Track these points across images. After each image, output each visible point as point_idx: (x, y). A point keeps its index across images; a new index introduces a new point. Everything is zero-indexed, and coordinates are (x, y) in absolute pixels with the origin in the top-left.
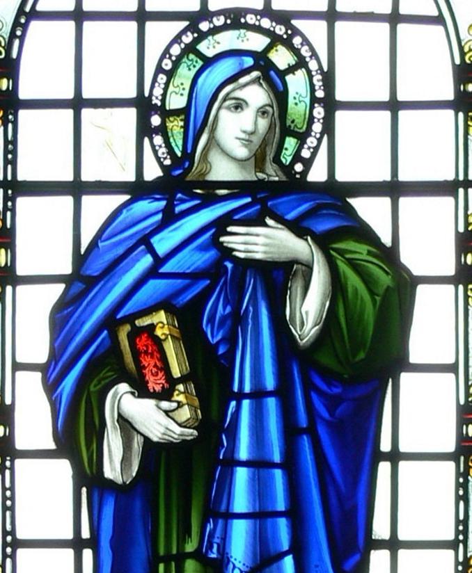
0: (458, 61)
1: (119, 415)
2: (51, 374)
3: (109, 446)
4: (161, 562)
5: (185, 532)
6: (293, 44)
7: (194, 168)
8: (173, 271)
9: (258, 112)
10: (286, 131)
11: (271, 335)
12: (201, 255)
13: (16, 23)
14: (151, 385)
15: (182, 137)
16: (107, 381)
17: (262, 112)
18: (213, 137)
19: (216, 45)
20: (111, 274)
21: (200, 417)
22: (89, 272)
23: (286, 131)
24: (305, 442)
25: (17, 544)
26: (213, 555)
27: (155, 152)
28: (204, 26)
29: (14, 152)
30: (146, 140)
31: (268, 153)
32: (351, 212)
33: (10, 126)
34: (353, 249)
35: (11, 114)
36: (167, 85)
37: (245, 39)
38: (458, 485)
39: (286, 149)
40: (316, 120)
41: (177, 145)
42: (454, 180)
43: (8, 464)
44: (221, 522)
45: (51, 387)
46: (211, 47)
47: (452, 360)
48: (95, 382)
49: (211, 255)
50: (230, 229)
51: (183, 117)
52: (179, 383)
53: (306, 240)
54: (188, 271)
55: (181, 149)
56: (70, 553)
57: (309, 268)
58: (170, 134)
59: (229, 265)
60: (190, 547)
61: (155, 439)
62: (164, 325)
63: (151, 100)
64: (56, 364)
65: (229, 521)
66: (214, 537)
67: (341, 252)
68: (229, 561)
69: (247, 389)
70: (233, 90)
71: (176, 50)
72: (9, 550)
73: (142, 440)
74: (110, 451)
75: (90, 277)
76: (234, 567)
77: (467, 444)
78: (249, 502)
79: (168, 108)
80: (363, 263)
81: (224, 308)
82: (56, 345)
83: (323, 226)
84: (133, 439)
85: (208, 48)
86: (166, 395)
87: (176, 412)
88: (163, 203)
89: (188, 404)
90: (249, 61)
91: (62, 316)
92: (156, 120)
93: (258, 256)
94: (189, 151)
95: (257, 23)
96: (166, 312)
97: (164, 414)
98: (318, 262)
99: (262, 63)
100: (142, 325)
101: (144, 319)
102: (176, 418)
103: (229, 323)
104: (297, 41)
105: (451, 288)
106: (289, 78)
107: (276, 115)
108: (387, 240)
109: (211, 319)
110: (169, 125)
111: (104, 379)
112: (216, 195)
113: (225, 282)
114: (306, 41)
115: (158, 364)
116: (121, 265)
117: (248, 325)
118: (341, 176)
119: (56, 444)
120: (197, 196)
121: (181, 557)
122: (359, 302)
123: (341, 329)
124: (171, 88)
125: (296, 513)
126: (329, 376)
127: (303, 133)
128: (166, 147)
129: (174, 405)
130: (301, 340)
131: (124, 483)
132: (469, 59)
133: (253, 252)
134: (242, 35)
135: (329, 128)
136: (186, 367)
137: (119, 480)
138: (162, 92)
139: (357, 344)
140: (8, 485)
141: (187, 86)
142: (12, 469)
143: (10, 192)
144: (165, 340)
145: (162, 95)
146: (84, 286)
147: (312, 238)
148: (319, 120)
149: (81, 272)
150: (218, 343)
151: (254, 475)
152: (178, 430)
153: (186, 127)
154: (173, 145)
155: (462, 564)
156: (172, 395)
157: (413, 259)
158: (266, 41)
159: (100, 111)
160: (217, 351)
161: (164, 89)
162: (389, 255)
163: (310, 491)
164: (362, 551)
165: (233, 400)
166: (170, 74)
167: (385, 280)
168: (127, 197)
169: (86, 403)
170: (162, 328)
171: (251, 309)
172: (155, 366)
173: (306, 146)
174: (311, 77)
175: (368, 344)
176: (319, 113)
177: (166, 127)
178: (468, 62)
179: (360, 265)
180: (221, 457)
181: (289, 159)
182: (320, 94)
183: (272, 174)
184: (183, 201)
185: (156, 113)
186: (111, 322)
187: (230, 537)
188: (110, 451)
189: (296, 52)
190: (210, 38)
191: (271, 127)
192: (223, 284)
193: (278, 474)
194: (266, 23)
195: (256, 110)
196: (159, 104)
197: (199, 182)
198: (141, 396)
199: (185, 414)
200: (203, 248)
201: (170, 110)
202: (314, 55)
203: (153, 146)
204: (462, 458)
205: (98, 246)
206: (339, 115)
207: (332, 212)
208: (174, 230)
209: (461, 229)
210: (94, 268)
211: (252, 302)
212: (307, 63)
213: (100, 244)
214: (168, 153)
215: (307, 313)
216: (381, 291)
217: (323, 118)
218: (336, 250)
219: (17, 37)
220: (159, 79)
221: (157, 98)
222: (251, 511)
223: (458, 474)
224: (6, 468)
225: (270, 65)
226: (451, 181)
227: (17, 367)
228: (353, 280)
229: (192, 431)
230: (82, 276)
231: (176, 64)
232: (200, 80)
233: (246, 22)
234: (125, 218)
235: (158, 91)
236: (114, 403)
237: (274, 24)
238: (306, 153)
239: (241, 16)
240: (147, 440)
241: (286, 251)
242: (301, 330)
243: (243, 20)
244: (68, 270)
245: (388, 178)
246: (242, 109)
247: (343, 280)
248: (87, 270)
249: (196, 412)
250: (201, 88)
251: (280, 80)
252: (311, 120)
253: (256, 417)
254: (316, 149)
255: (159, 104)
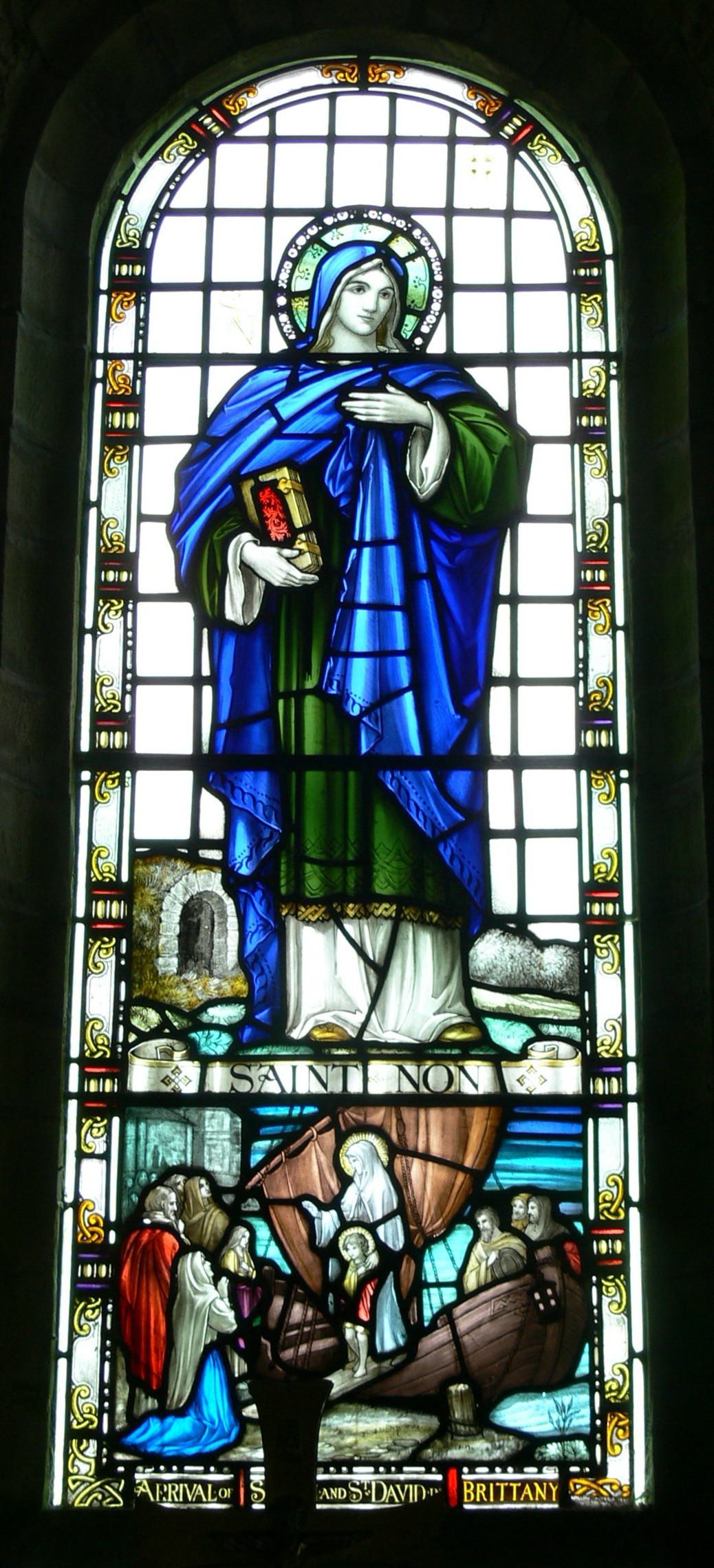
0: (570, 250)
1: (242, 562)
2: (176, 524)
3: (231, 590)
4: (281, 698)
5: (305, 669)
6: (413, 236)
7: (318, 342)
8: (297, 432)
9: (379, 293)
10: (406, 310)
11: (391, 489)
12: (323, 419)
13: (151, 219)
14: (273, 535)
15: (306, 315)
16: (230, 531)
17: (383, 293)
18: (337, 315)
19: (340, 236)
20: (237, 435)
21: (321, 563)
22: (214, 434)
23: (406, 310)
24: (425, 587)
25: (137, 681)
26: (334, 691)
27: (281, 328)
28: (329, 221)
29: (146, 329)
30: (272, 318)
31: (389, 328)
32: (469, 380)
33: (142, 306)
34: (471, 412)
35: (143, 295)
36: (293, 270)
37: (367, 232)
38: (577, 626)
39: (406, 325)
40: (435, 300)
41: (302, 323)
42: (568, 352)
43: (130, 606)
44: (341, 661)
45: (175, 537)
46: (335, 238)
47: (569, 512)
48: (218, 531)
49: (333, 418)
50: (351, 395)
51: (307, 298)
52: (301, 533)
53: (426, 405)
54: (311, 432)
55: (305, 325)
56: (190, 690)
57: (428, 430)
58: (295, 313)
59: (351, 427)
60: (310, 684)
61: (277, 584)
62: (287, 480)
63: (278, 284)
64: (180, 516)
65: (349, 659)
66: (334, 675)
67: (458, 415)
68: (348, 697)
69: (368, 538)
70: (356, 275)
71: (301, 241)
72: (129, 687)
73: (264, 584)
74: (231, 594)
75: (215, 437)
76: (354, 702)
77: (585, 588)
78: (369, 641)
79: (293, 290)
80: (481, 425)
81: (346, 465)
82: (181, 498)
83: (442, 392)
84: (255, 583)
85: (331, 239)
86: (288, 543)
87: (298, 559)
88: (287, 373)
89: (309, 552)
90: (371, 250)
91: (187, 474)
92: (282, 301)
93: (379, 419)
94: (313, 327)
95: (379, 218)
96: (289, 469)
97: (285, 560)
98: (437, 424)
99: (383, 252)
100: (265, 480)
101: (268, 475)
102: (297, 564)
103: (350, 478)
104: (417, 233)
105: (567, 447)
106: (409, 265)
107: (397, 296)
108: (504, 404)
109: (333, 476)
110: (294, 305)
111: (227, 529)
112: (339, 365)
113: (347, 442)
114: (425, 233)
115: (280, 515)
116: (246, 427)
117: (369, 480)
118: (459, 348)
119: (179, 589)
120: (321, 366)
121: (301, 694)
122: (477, 460)
123: (460, 484)
124: (296, 273)
125: (416, 652)
126: (447, 525)
127: (422, 311)
128: (291, 324)
129: (296, 552)
130: (421, 493)
131: (245, 624)
132: (581, 248)
133: (375, 415)
134: (365, 228)
135: (447, 307)
136: (308, 519)
137: (241, 622)
138: (288, 276)
139: (475, 498)
140: (130, 625)
141: (312, 271)
142: (134, 611)
143: (140, 363)
144: (287, 494)
145: (288, 279)
146: (210, 446)
147: (431, 403)
148: (438, 300)
149: (207, 434)
150: (340, 496)
151: (374, 616)
152: (299, 575)
153: (310, 307)
154: (298, 322)
155: (582, 700)
156: (294, 544)
157: (529, 420)
158: (387, 233)
159: (228, 293)
160: (339, 503)
161: (289, 274)
162: (507, 418)
163: (430, 631)
164: (482, 687)
165: (354, 548)
166: (296, 262)
167: (502, 439)
168: (253, 367)
169: (209, 550)
170: (285, 483)
171: (372, 466)
172: (278, 517)
173: (425, 323)
174: (429, 263)
175: (487, 497)
176: (438, 295)
177: (291, 307)
178: (579, 250)
179: (478, 427)
180: (342, 600)
181: (409, 334)
182: (439, 278)
183: (393, 347)
184: (306, 371)
185: (282, 295)
186: (235, 477)
187: (350, 675)
188: (231, 594)
189: (416, 242)
190: (334, 230)
191: (392, 307)
192: (345, 444)
193: (398, 616)
194: (387, 218)
195: (377, 292)
196: (285, 286)
197: (322, 354)
198: (263, 544)
199: (307, 560)
200: (325, 412)
201: (295, 292)
202: (433, 245)
203: (279, 323)
204: (581, 602)
205: (224, 410)
206: (458, 297)
207: (451, 380)
208: (296, 397)
209: (576, 395)
210: (220, 429)
211: (372, 459)
212: (426, 251)
213: (226, 409)
214: (293, 329)
215: (426, 469)
216: (499, 449)
217: (442, 299)
218: (455, 414)
219: (151, 230)
220: (285, 266)
221: (283, 282)
222: (371, 650)
223: (577, 616)
224: (128, 610)
225: (393, 254)
226: (565, 353)
227: (142, 518)
228: (471, 440)
229: (312, 576)
230: (208, 437)
231: (302, 252)
232: (325, 267)
233: (368, 217)
234: (250, 386)
235: (284, 276)
236: (237, 551)
237: (395, 219)
238: (425, 329)
239: (364, 212)
240: (269, 585)
241: (406, 414)
242: (421, 485)
243: (365, 216)
244: (193, 429)
245: (505, 350)
246: (364, 291)
247: (461, 439)
248: (213, 431)
249: (317, 559)
250: (326, 273)
251: (401, 266)
252: (430, 300)
253: (376, 563)
254: (435, 326)
255: (285, 286)
